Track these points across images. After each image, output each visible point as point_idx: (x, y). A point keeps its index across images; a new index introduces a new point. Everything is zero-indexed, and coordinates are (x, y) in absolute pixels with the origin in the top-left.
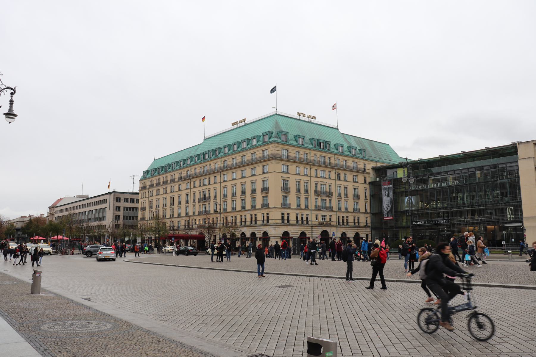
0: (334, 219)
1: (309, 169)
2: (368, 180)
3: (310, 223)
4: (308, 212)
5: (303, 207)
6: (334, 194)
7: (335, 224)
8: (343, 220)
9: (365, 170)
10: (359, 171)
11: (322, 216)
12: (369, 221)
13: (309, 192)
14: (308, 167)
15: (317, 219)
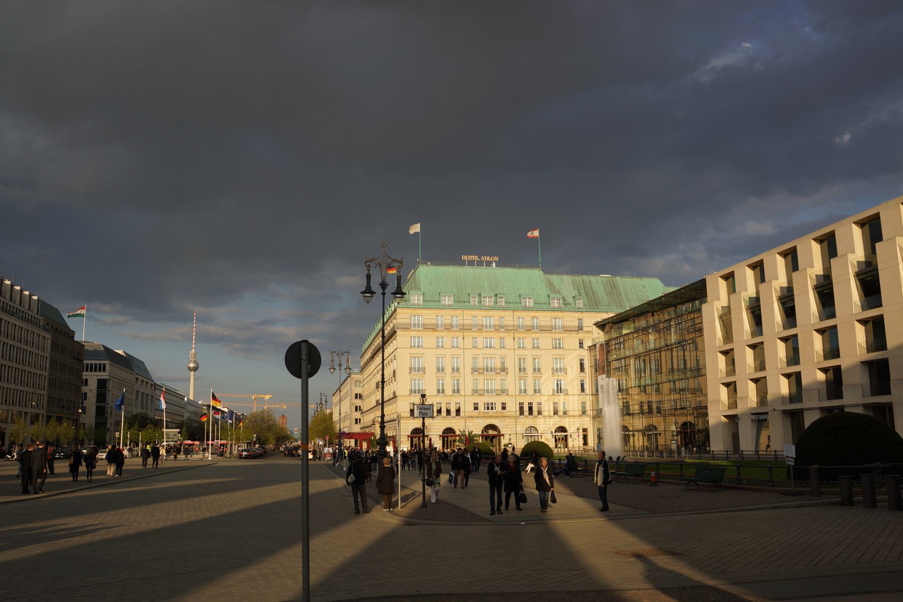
0: (512, 407)
1: (460, 339)
2: (588, 343)
3: (462, 414)
4: (459, 399)
5: (448, 391)
6: (511, 371)
7: (514, 414)
8: (531, 409)
9: (580, 328)
10: (567, 330)
11: (488, 404)
12: (588, 407)
13: (461, 371)
14: (460, 334)
15: (476, 409)
